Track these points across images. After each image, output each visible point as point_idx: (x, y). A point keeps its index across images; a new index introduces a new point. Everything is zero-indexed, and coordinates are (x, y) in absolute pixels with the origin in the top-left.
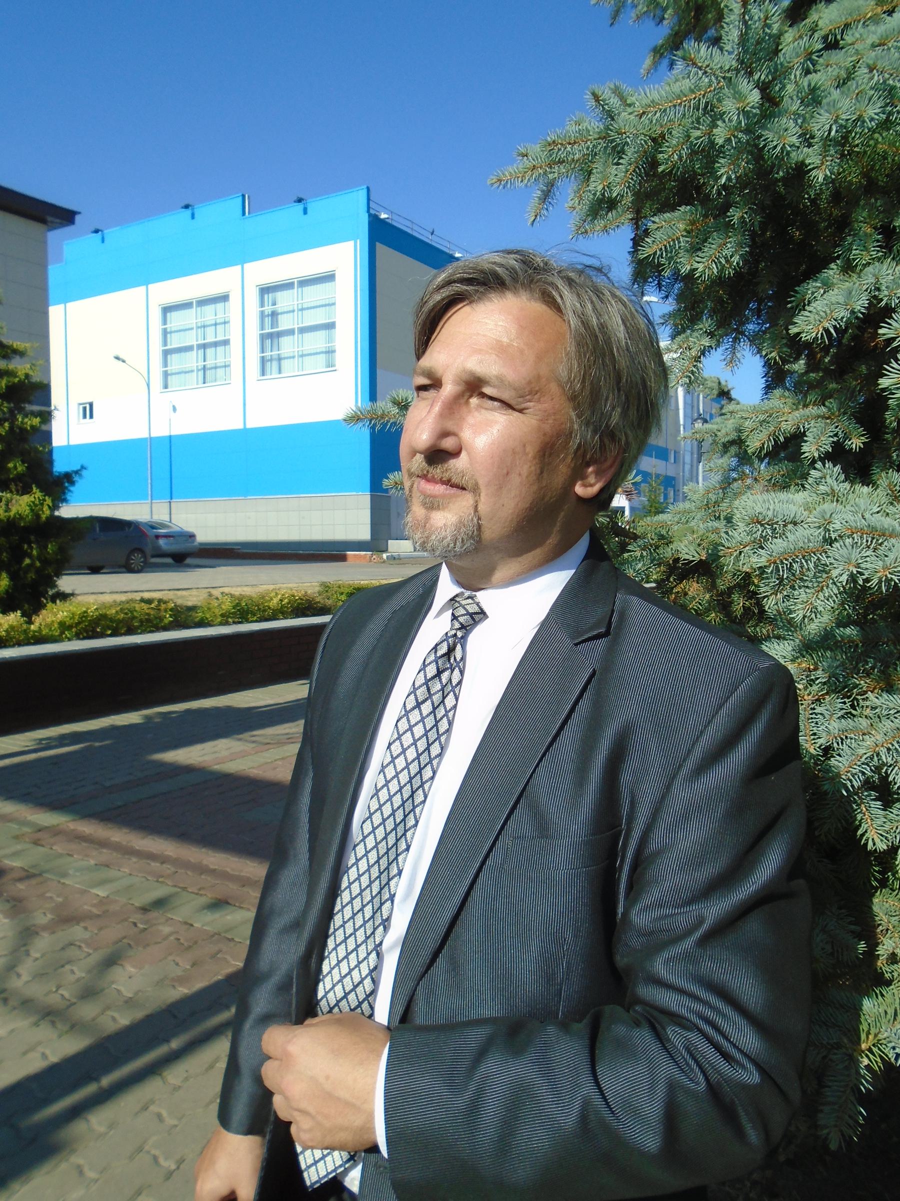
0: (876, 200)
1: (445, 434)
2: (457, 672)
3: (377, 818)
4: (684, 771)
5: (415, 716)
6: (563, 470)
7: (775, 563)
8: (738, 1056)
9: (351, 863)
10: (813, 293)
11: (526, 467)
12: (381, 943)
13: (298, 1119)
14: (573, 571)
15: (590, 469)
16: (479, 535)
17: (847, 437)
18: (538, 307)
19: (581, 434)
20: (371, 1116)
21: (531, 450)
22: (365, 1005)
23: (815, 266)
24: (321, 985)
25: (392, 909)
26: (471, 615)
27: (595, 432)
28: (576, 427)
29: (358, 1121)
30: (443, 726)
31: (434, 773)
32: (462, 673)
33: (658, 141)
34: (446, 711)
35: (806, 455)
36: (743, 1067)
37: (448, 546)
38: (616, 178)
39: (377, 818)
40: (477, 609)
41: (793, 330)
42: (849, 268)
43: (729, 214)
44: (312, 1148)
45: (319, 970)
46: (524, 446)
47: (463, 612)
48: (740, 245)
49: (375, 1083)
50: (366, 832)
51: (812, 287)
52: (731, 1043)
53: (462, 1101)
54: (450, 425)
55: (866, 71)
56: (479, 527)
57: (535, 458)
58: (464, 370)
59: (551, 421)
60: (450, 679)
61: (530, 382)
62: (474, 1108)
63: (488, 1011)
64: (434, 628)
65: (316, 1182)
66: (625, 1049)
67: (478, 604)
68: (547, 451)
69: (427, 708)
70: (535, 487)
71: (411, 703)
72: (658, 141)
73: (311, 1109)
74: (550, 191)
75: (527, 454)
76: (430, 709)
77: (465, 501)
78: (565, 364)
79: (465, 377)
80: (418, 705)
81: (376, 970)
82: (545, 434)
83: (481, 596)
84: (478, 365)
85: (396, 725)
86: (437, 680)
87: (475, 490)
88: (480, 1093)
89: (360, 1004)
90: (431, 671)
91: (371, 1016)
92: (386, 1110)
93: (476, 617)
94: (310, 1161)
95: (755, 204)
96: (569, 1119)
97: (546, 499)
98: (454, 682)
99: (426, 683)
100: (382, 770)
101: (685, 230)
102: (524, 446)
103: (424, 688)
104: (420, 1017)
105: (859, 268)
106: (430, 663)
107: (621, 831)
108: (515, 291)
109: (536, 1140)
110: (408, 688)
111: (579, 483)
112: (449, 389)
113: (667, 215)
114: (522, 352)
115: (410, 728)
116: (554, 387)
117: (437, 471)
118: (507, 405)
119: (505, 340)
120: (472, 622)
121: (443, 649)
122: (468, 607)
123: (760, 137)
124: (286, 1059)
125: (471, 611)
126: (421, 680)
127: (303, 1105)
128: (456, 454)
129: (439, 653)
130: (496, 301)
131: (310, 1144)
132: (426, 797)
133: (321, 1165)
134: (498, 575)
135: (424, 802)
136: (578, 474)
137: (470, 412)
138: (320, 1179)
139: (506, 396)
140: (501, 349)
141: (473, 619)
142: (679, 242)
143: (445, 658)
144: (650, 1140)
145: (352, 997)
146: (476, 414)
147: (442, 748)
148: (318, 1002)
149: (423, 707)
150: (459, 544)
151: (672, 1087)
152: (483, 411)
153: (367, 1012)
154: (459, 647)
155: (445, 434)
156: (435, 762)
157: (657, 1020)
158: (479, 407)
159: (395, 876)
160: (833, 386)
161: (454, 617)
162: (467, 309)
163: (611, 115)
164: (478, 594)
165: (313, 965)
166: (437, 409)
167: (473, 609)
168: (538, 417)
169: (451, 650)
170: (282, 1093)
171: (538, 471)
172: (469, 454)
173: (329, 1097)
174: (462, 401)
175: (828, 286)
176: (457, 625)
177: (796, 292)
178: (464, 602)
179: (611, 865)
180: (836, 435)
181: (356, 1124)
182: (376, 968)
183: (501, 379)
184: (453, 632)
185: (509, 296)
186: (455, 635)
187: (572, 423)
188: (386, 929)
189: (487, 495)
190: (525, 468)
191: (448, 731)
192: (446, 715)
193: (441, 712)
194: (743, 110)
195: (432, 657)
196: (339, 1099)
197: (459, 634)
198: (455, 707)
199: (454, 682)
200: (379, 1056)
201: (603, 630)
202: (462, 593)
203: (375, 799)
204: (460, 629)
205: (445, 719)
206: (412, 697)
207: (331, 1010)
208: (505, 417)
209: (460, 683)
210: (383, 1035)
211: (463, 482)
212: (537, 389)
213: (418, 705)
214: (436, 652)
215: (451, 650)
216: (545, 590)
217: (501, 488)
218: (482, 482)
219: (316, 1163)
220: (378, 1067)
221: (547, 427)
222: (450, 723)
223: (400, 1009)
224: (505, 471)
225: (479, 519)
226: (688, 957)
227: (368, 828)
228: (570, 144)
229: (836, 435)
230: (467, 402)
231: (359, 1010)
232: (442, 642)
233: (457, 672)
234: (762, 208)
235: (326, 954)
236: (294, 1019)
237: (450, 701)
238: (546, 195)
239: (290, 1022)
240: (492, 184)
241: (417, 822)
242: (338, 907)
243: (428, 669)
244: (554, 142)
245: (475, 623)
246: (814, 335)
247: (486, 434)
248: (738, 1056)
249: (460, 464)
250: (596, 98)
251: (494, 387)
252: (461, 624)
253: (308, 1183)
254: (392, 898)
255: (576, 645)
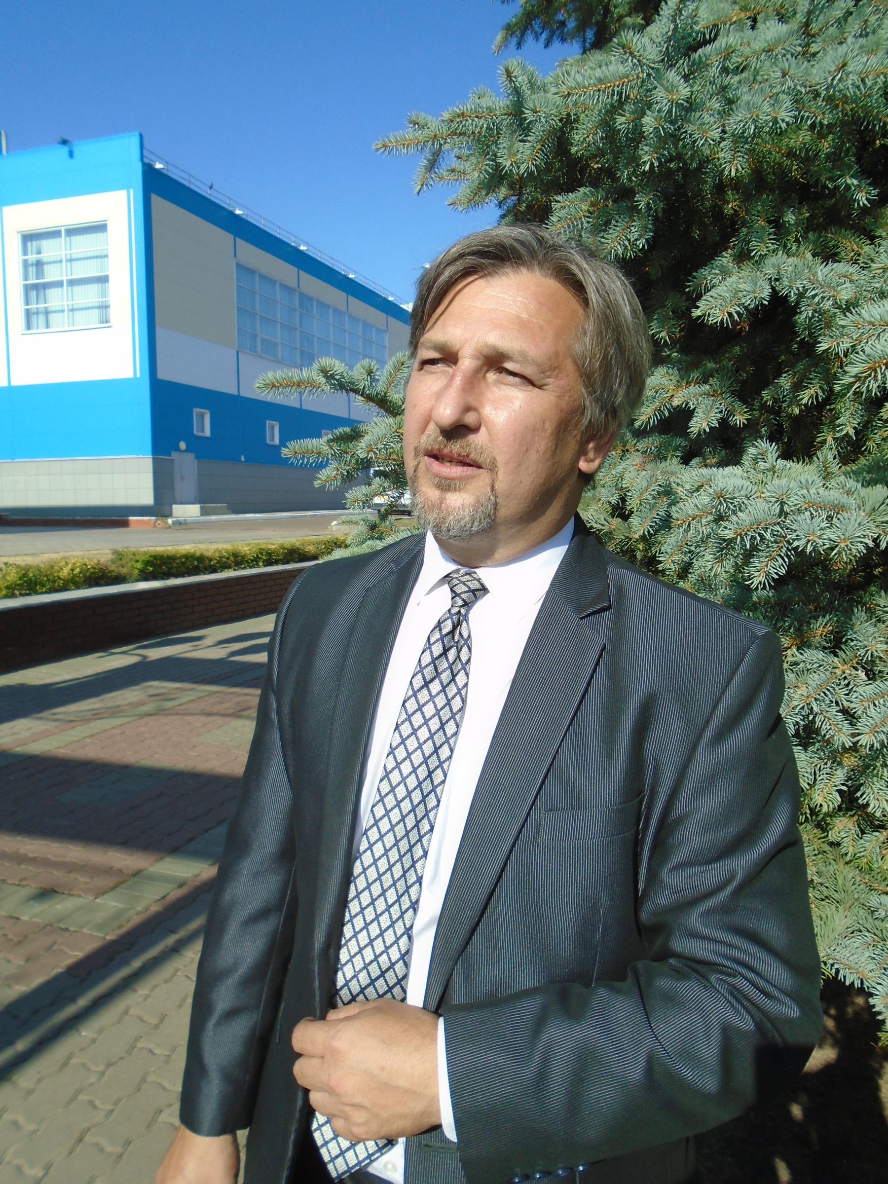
0: (768, 195)
1: (468, 409)
2: (465, 649)
3: (390, 801)
4: (708, 734)
5: (423, 696)
6: (572, 445)
7: (741, 535)
8: (776, 993)
9: (362, 848)
10: (711, 281)
11: (543, 444)
12: (412, 927)
13: (351, 1113)
14: (567, 546)
15: (591, 445)
16: (495, 514)
17: (731, 413)
18: (552, 284)
19: (592, 412)
20: (435, 1100)
21: (549, 427)
22: (397, 990)
23: (705, 254)
24: (340, 975)
25: (420, 891)
26: (473, 592)
27: (602, 409)
28: (587, 403)
29: (417, 1106)
30: (457, 704)
31: (452, 751)
32: (470, 649)
33: (569, 122)
34: (458, 688)
35: (692, 429)
36: (779, 1001)
37: (465, 526)
38: (522, 155)
39: (390, 801)
40: (478, 586)
41: (696, 313)
42: (743, 257)
43: (636, 199)
44: (364, 1140)
45: (338, 959)
46: (544, 423)
47: (465, 589)
48: (645, 228)
49: (436, 1067)
50: (378, 816)
51: (707, 274)
52: (768, 982)
53: (530, 1070)
54: (472, 401)
55: (779, 74)
56: (496, 504)
57: (552, 434)
58: (486, 345)
59: (567, 398)
60: (459, 656)
61: (550, 359)
62: (542, 1077)
63: (527, 980)
64: (425, 607)
65: (345, 1173)
66: (671, 999)
67: (479, 580)
68: (563, 426)
69: (435, 687)
70: (549, 464)
71: (418, 682)
72: (569, 122)
73: (366, 1102)
74: (435, 161)
75: (545, 431)
76: (440, 688)
77: (482, 479)
78: (586, 343)
79: (486, 351)
80: (426, 684)
81: (405, 957)
82: (562, 411)
83: (483, 573)
84: (496, 339)
85: (403, 705)
86: (443, 658)
87: (492, 468)
88: (545, 1062)
89: (390, 989)
90: (437, 649)
91: (404, 1000)
92: (452, 1093)
93: (477, 593)
94: (335, 1151)
95: (658, 191)
96: (636, 1073)
97: (558, 474)
98: (464, 660)
99: (434, 660)
100: (392, 751)
101: (588, 211)
102: (544, 423)
103: (431, 667)
104: (458, 997)
105: (756, 258)
106: (435, 642)
107: (644, 796)
108: (529, 268)
109: (603, 1097)
110: (412, 666)
111: (583, 458)
112: (467, 363)
113: (571, 196)
114: (541, 328)
115: (420, 708)
116: (569, 366)
117: (455, 448)
118: (528, 381)
119: (524, 316)
120: (473, 599)
121: (447, 627)
122: (469, 584)
123: (679, 128)
124: (330, 1056)
125: (473, 587)
126: (427, 659)
127: (357, 1100)
128: (475, 430)
129: (444, 632)
130: (512, 276)
131: (364, 1137)
132: (445, 775)
133: (350, 1155)
134: (500, 554)
135: (443, 782)
136: (582, 452)
137: (488, 387)
138: (349, 1169)
139: (528, 371)
140: (522, 325)
141: (475, 595)
142: (582, 224)
143: (450, 636)
144: (709, 1083)
145: (380, 983)
146: (495, 389)
147: (458, 726)
148: (337, 992)
149: (431, 686)
150: (476, 524)
151: (727, 1030)
152: (503, 387)
153: (399, 998)
154: (464, 624)
155: (468, 409)
156: (452, 741)
157: (698, 968)
158: (498, 382)
159: (420, 858)
160: (711, 365)
161: (455, 595)
162: (481, 283)
163: (517, 91)
164: (477, 570)
165: (332, 956)
166: (458, 381)
167: (474, 585)
168: (556, 394)
169: (456, 625)
170: (331, 1091)
171: (554, 448)
172: (488, 431)
173: (386, 1087)
174: (481, 375)
175: (725, 273)
176: (460, 602)
177: (694, 277)
178: (463, 579)
179: (640, 830)
180: (721, 412)
181: (416, 1110)
182: (407, 952)
183: (524, 356)
184: (457, 609)
185: (524, 270)
186: (459, 612)
187: (584, 399)
188: (415, 911)
189: (505, 472)
190: (542, 444)
191: (461, 709)
192: (459, 692)
193: (452, 690)
194: (677, 103)
195: (437, 636)
196: (397, 1088)
197: (463, 611)
198: (466, 685)
199: (464, 660)
200: (434, 1039)
201: (607, 604)
202: (458, 571)
203: (385, 782)
204: (462, 606)
205: (458, 697)
206: (419, 676)
207: (353, 999)
208: (526, 393)
209: (469, 661)
210: (428, 1018)
211: (481, 460)
212: (556, 364)
213: (426, 684)
214: (440, 630)
215: (456, 625)
216: (547, 563)
217: (520, 465)
218: (500, 460)
219: (342, 1153)
220: (436, 1050)
221: (564, 404)
222: (464, 701)
223: (439, 990)
224: (525, 448)
225: (496, 497)
226: (725, 909)
227: (379, 811)
228: (477, 117)
229: (721, 412)
230: (484, 376)
231: (389, 995)
232: (445, 620)
233: (465, 649)
234: (665, 196)
235: (343, 942)
236: (318, 1013)
237: (461, 679)
238: (432, 165)
239: (315, 1016)
240: (377, 150)
241: (439, 801)
242: (352, 893)
243: (434, 648)
244: (463, 113)
245: (476, 598)
246: (720, 319)
247: (507, 409)
248: (776, 993)
249: (479, 439)
250: (509, 74)
251: (517, 362)
252: (464, 601)
253: (334, 1174)
254: (419, 880)
255: (582, 619)
